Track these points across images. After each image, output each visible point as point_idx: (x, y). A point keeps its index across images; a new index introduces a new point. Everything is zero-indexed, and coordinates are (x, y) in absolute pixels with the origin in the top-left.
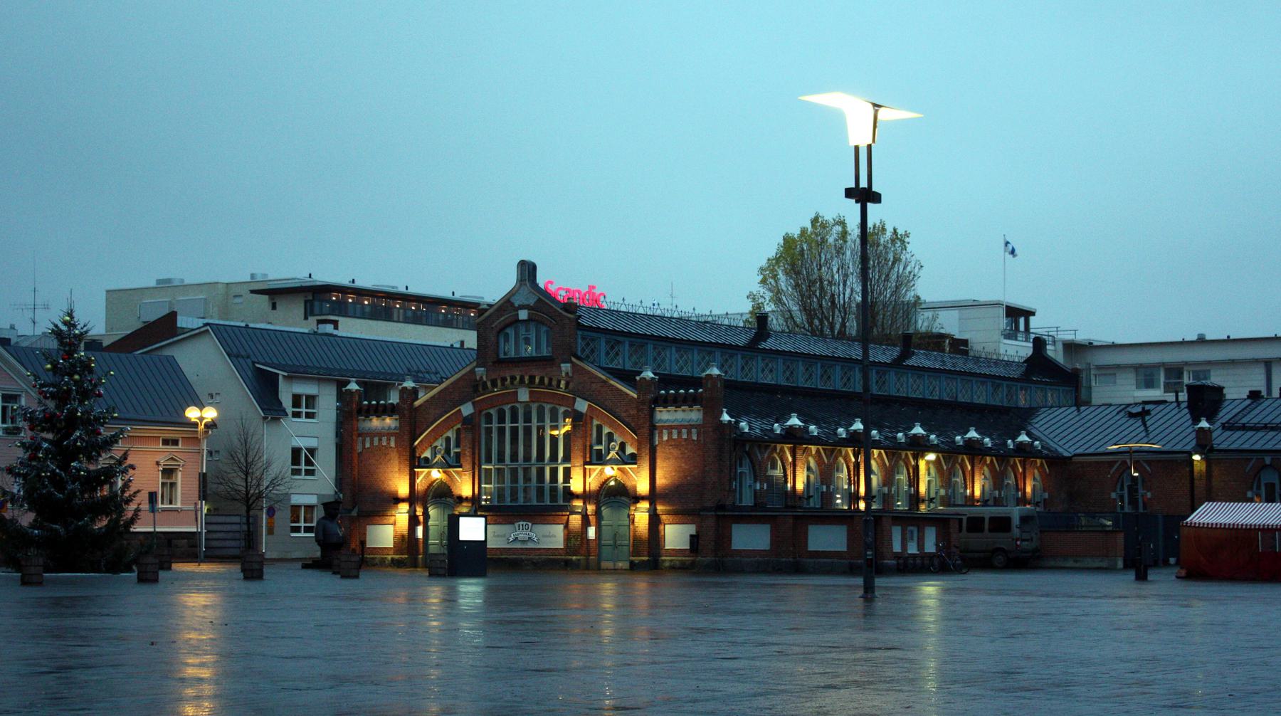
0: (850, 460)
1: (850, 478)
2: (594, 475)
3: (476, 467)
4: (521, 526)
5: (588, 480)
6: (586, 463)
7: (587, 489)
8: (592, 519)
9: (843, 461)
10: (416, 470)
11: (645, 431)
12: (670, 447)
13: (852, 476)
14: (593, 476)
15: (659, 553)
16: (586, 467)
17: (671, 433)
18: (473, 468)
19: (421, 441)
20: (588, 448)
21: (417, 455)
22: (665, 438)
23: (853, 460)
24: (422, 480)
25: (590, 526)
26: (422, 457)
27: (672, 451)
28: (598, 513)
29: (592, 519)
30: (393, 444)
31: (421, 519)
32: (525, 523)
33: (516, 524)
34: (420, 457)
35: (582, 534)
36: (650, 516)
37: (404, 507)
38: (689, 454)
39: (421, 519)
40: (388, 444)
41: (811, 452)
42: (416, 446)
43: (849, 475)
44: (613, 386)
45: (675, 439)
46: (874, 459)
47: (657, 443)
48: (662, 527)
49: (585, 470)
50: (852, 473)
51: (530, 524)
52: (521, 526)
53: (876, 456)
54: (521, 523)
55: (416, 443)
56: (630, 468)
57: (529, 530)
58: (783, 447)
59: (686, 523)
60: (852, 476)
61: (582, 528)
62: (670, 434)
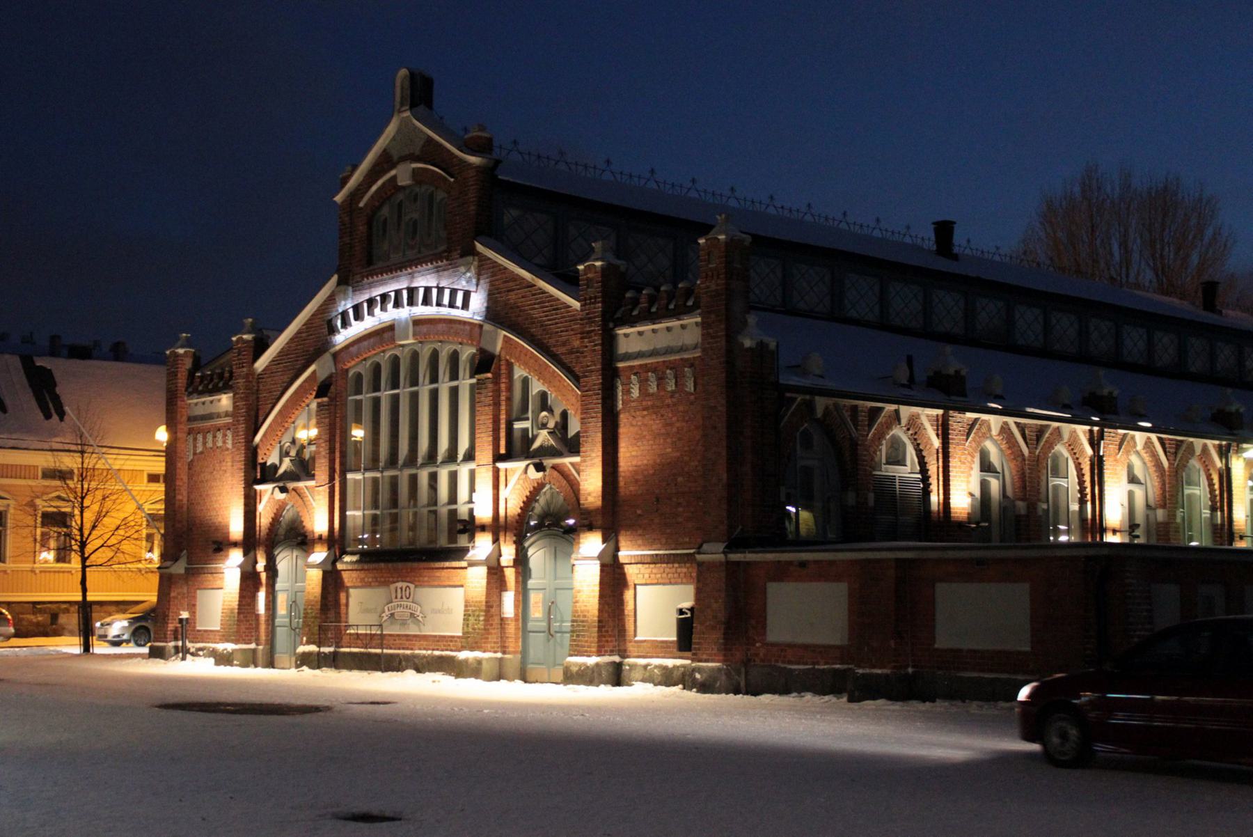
0: (1083, 451)
1: (1082, 490)
2: (513, 480)
3: (337, 477)
4: (399, 591)
5: (503, 493)
6: (498, 458)
7: (502, 512)
8: (510, 574)
9: (1066, 454)
10: (258, 487)
11: (595, 379)
12: (645, 413)
13: (1088, 484)
14: (510, 485)
15: (625, 651)
16: (501, 465)
17: (647, 380)
18: (332, 479)
19: (264, 435)
20: (503, 426)
21: (260, 461)
22: (635, 393)
23: (1089, 451)
24: (265, 506)
25: (506, 590)
26: (268, 464)
27: (646, 420)
28: (521, 561)
29: (510, 574)
30: (229, 445)
31: (263, 576)
32: (404, 585)
33: (393, 587)
34: (265, 463)
35: (489, 606)
36: (603, 566)
37: (236, 557)
38: (678, 425)
39: (263, 576)
40: (224, 442)
41: (989, 429)
42: (257, 446)
43: (1081, 483)
44: (544, 292)
45: (653, 394)
46: (1138, 453)
47: (620, 406)
48: (628, 595)
49: (496, 473)
50: (1087, 478)
51: (412, 586)
52: (399, 591)
53: (1139, 447)
54: (399, 585)
55: (258, 438)
56: (572, 464)
57: (411, 599)
58: (918, 416)
59: (670, 583)
60: (1088, 484)
61: (488, 594)
62: (643, 383)
